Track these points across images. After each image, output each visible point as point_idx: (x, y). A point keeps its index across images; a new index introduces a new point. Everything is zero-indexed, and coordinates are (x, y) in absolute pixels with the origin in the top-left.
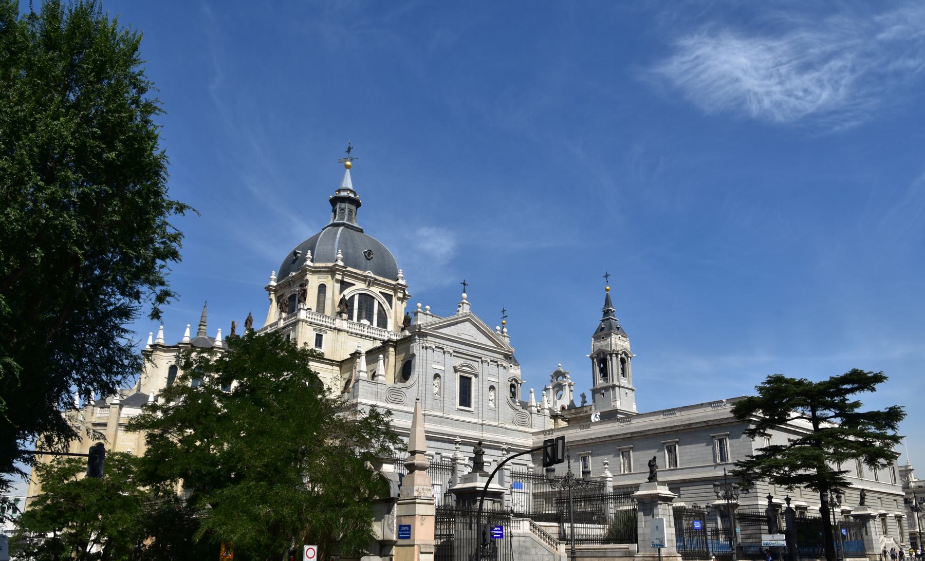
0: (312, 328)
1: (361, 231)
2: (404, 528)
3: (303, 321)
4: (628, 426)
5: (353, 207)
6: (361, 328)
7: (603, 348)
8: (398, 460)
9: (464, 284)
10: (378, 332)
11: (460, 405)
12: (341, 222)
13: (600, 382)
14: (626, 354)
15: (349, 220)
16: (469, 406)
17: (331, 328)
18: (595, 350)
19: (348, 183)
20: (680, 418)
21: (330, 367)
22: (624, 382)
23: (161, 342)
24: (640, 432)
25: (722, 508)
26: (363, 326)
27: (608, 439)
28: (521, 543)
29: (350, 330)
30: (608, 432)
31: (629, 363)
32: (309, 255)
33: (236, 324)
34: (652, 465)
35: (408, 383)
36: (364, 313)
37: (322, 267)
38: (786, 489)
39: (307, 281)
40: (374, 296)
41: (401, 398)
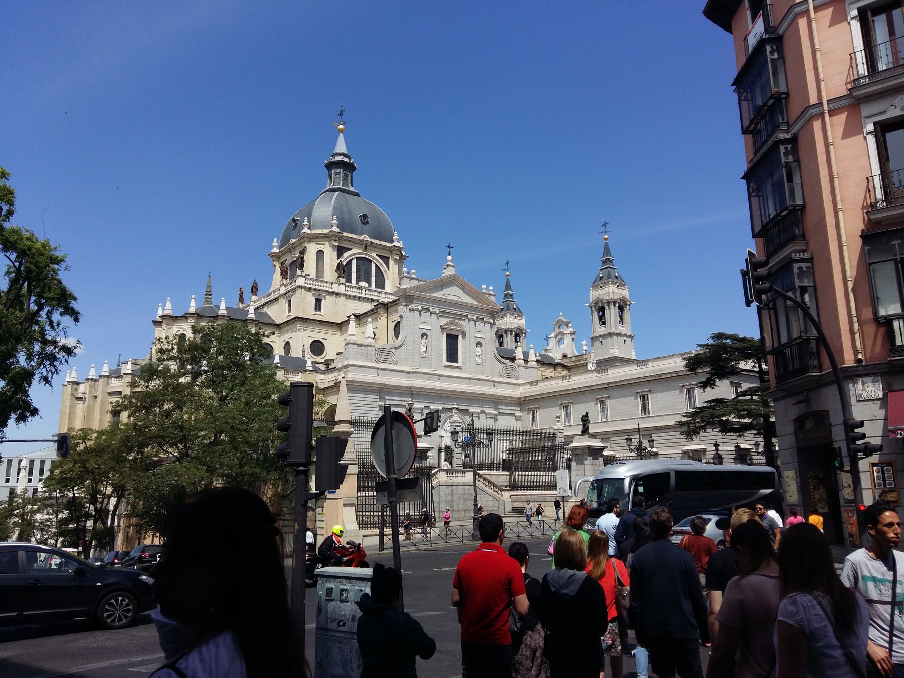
1: (357, 195)
4: (605, 377)
6: (359, 291)
7: (602, 297)
8: (357, 423)
11: (447, 361)
15: (345, 184)
16: (457, 362)
19: (341, 146)
20: (652, 368)
23: (170, 313)
24: (616, 382)
25: (691, 454)
26: (361, 288)
28: (466, 491)
29: (348, 293)
30: (587, 382)
31: (627, 314)
32: (306, 222)
33: (243, 290)
34: (585, 420)
36: (362, 277)
38: (755, 435)
40: (371, 259)
41: (390, 357)
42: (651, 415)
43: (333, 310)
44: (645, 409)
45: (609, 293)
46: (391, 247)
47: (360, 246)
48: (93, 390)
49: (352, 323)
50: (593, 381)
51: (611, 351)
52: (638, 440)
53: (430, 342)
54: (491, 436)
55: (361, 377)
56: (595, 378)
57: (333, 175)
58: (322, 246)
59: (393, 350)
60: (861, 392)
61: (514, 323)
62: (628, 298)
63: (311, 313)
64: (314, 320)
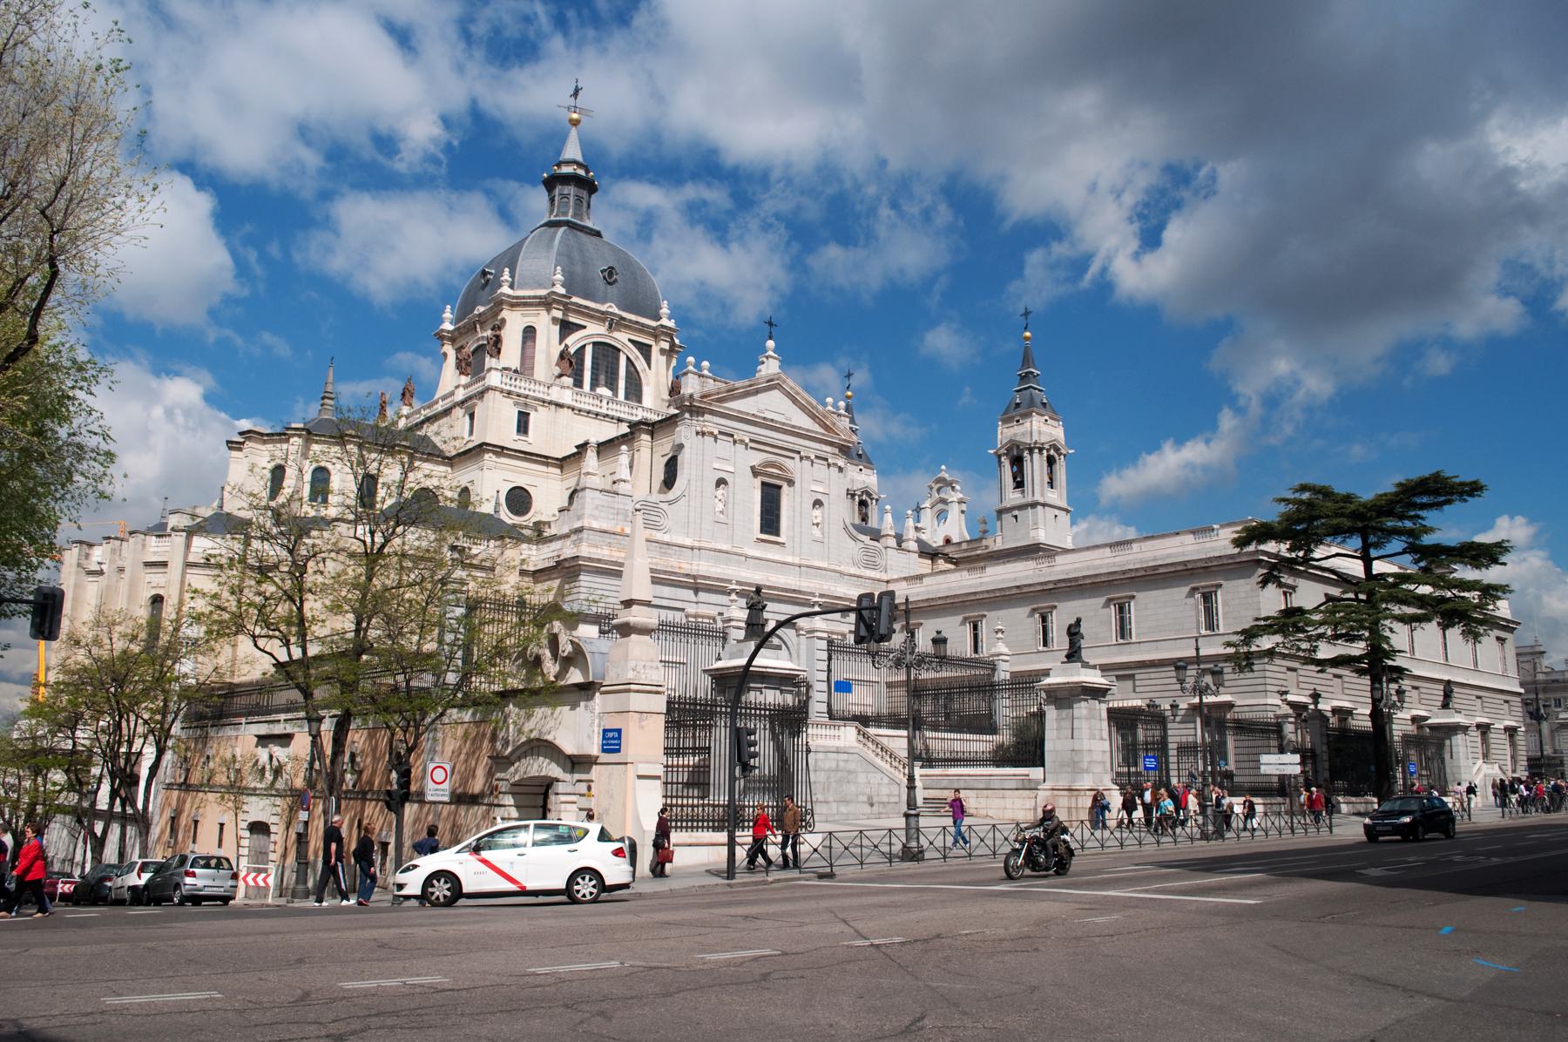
0: (510, 402)
1: (598, 234)
2: (610, 735)
3: (494, 389)
5: (585, 194)
6: (597, 402)
7: (1018, 439)
9: (771, 324)
10: (626, 409)
11: (761, 532)
12: (562, 218)
13: (1011, 496)
14: (1057, 450)
16: (778, 534)
17: (544, 402)
18: (1004, 442)
20: (1139, 556)
21: (544, 468)
22: (1053, 497)
24: (1069, 580)
26: (600, 398)
27: (1014, 591)
28: (841, 764)
29: (578, 405)
30: (1015, 580)
32: (506, 276)
34: (1074, 632)
35: (671, 495)
36: (602, 378)
37: (529, 297)
39: (503, 321)
41: (658, 519)
42: (1134, 640)
44: (1123, 631)
45: (1031, 433)
46: (654, 328)
48: (117, 558)
49: (591, 455)
50: (1027, 577)
51: (1032, 533)
53: (731, 495)
54: (942, 646)
56: (1031, 572)
57: (556, 198)
61: (857, 481)
63: (509, 437)
64: (516, 451)
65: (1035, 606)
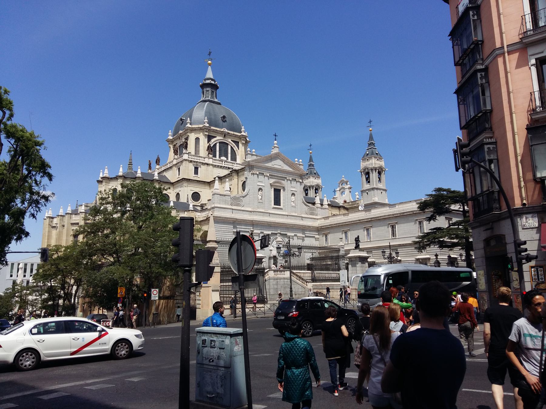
1: (219, 104)
3: (186, 160)
4: (369, 214)
6: (221, 162)
7: (368, 166)
8: (220, 242)
12: (207, 99)
15: (212, 97)
19: (210, 74)
20: (398, 209)
23: (107, 175)
24: (376, 218)
26: (222, 161)
28: (285, 282)
29: (214, 164)
30: (358, 218)
31: (383, 176)
32: (188, 121)
34: (357, 240)
38: (460, 249)
40: (228, 143)
41: (240, 202)
43: (205, 174)
44: (393, 234)
45: (372, 164)
47: (221, 135)
48: (62, 222)
49: (217, 182)
50: (362, 217)
51: (373, 199)
52: (389, 252)
53: (264, 193)
54: (300, 250)
55: (222, 214)
56: (363, 215)
57: (205, 92)
58: (198, 135)
59: (242, 198)
60: (525, 224)
62: (384, 167)
63: (192, 176)
64: (194, 180)
65: (365, 226)
